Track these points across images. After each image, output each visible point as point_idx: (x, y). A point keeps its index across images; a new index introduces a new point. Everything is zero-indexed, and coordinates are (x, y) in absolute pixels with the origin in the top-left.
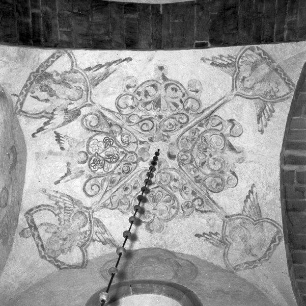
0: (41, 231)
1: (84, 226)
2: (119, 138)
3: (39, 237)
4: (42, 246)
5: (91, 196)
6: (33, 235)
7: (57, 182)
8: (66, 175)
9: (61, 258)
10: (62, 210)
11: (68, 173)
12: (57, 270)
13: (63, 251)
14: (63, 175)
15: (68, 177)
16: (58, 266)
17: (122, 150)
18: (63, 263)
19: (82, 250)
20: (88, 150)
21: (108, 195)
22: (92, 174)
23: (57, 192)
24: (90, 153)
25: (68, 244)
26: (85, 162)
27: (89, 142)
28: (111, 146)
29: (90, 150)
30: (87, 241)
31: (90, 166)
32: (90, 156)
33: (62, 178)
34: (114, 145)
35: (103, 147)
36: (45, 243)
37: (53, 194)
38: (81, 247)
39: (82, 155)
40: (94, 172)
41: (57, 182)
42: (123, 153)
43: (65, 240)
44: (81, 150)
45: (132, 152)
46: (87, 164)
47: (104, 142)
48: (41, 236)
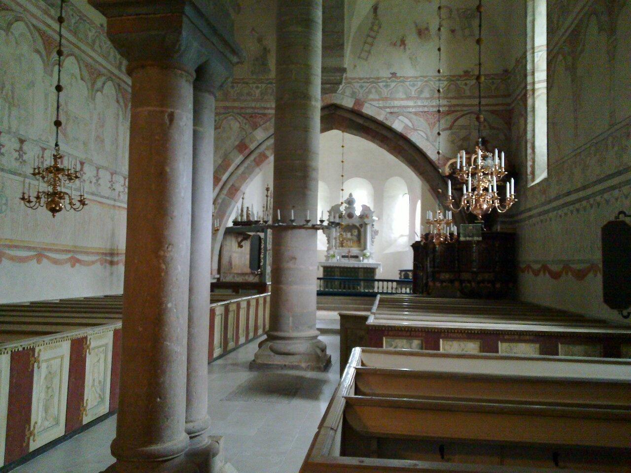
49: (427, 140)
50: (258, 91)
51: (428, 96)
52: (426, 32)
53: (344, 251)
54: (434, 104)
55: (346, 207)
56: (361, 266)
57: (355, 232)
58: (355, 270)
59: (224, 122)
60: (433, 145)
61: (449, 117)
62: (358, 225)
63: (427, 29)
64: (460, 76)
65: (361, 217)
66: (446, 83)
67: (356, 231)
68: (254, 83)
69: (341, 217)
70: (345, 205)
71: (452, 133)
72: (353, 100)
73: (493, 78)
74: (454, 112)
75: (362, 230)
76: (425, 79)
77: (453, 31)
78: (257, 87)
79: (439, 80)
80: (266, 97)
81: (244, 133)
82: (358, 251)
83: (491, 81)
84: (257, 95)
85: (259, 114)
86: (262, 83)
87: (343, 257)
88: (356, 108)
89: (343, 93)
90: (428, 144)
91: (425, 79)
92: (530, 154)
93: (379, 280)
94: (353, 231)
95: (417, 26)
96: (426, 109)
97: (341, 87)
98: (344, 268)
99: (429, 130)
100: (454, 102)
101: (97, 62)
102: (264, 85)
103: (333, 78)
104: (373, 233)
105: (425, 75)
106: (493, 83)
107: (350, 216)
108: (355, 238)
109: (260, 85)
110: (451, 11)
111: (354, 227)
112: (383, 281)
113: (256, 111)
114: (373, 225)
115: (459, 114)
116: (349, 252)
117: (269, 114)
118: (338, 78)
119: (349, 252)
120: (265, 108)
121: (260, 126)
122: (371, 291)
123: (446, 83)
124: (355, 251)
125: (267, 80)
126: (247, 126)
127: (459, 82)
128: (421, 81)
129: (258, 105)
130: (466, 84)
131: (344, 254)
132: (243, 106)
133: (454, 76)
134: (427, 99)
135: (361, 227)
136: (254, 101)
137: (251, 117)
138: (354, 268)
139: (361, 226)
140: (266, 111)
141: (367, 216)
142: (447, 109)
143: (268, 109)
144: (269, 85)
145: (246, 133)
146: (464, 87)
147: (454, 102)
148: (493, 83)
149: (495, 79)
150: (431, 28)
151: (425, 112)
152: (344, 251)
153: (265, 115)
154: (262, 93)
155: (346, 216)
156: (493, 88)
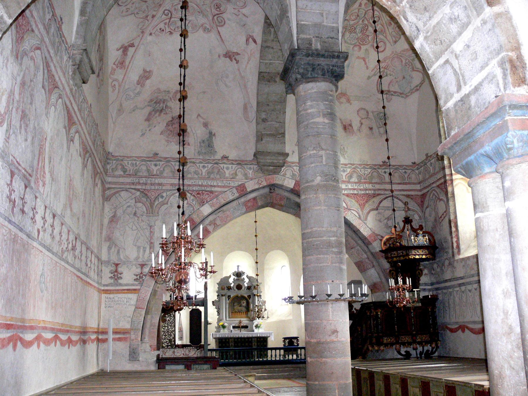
0: (392, 89)
1: (402, 61)
2: (352, 23)
3: (395, 92)
4: (401, 94)
5: (385, 49)
6: (392, 95)
7: (367, 68)
8: (364, 61)
9: (413, 85)
10: (386, 70)
11: (364, 59)
12: (418, 92)
13: (410, 82)
14: (364, 62)
15: (367, 60)
16: (417, 90)
17: (361, 21)
18: (417, 86)
19: (415, 71)
20: (353, 44)
21: (389, 37)
22: (370, 44)
23: (373, 69)
24: (355, 44)
25: (408, 77)
26: (360, 47)
27: (348, 43)
28: (355, 29)
29: (353, 43)
30: (412, 64)
31: (364, 45)
32: (358, 44)
33: (366, 64)
34: (355, 26)
35: (354, 34)
36: (399, 91)
37: (373, 73)
38: (413, 70)
39: (356, 48)
40: (369, 42)
41: (367, 68)
42: (363, 21)
43: (404, 78)
44: (351, 48)
45: (366, 13)
46: (362, 46)
47: (351, 33)
48: (394, 90)
49: (360, 218)
50: (204, 171)
51: (356, 181)
52: (350, 128)
53: (236, 321)
54: (362, 188)
55: (234, 279)
57: (244, 303)
59: (172, 197)
60: (365, 223)
61: (374, 199)
62: (246, 296)
63: (350, 125)
64: (380, 166)
65: (249, 288)
66: (369, 170)
67: (245, 301)
68: (201, 163)
69: (229, 288)
70: (233, 277)
71: (379, 213)
72: (294, 182)
73: (405, 169)
74: (378, 195)
75: (250, 301)
76: (353, 167)
77: (371, 129)
78: (204, 167)
79: (364, 168)
80: (212, 176)
81: (192, 209)
82: (248, 322)
83: (404, 171)
84: (204, 174)
85: (207, 191)
86: (208, 163)
87: (234, 327)
88: (297, 189)
89: (284, 175)
90: (361, 222)
91: (353, 167)
92: (454, 232)
93: (272, 349)
94: (242, 303)
95: (342, 123)
96: (356, 192)
97: (283, 169)
99: (360, 210)
100: (377, 187)
101: (86, 139)
102: (210, 165)
103: (276, 161)
105: (352, 163)
106: (405, 172)
107: (239, 287)
108: (244, 309)
109: (206, 165)
110: (367, 112)
111: (243, 297)
112: (276, 349)
113: (203, 188)
115: (382, 197)
116: (240, 322)
117: (216, 192)
118: (281, 161)
119: (240, 322)
120: (211, 186)
121: (207, 202)
123: (369, 170)
124: (245, 321)
125: (214, 160)
126: (194, 203)
127: (380, 170)
128: (349, 168)
129: (205, 183)
130: (385, 172)
131: (234, 325)
132: (190, 183)
133: (375, 165)
134: (356, 183)
135: (250, 298)
136: (201, 178)
137: (198, 194)
139: (249, 297)
140: (213, 189)
142: (373, 192)
143: (215, 186)
144: (216, 165)
145: (194, 209)
146: (384, 174)
147: (377, 187)
148: (405, 172)
149: (407, 169)
150: (353, 125)
151: (355, 194)
152: (236, 321)
153: (212, 192)
154: (209, 173)
155: (235, 288)
156: (406, 176)
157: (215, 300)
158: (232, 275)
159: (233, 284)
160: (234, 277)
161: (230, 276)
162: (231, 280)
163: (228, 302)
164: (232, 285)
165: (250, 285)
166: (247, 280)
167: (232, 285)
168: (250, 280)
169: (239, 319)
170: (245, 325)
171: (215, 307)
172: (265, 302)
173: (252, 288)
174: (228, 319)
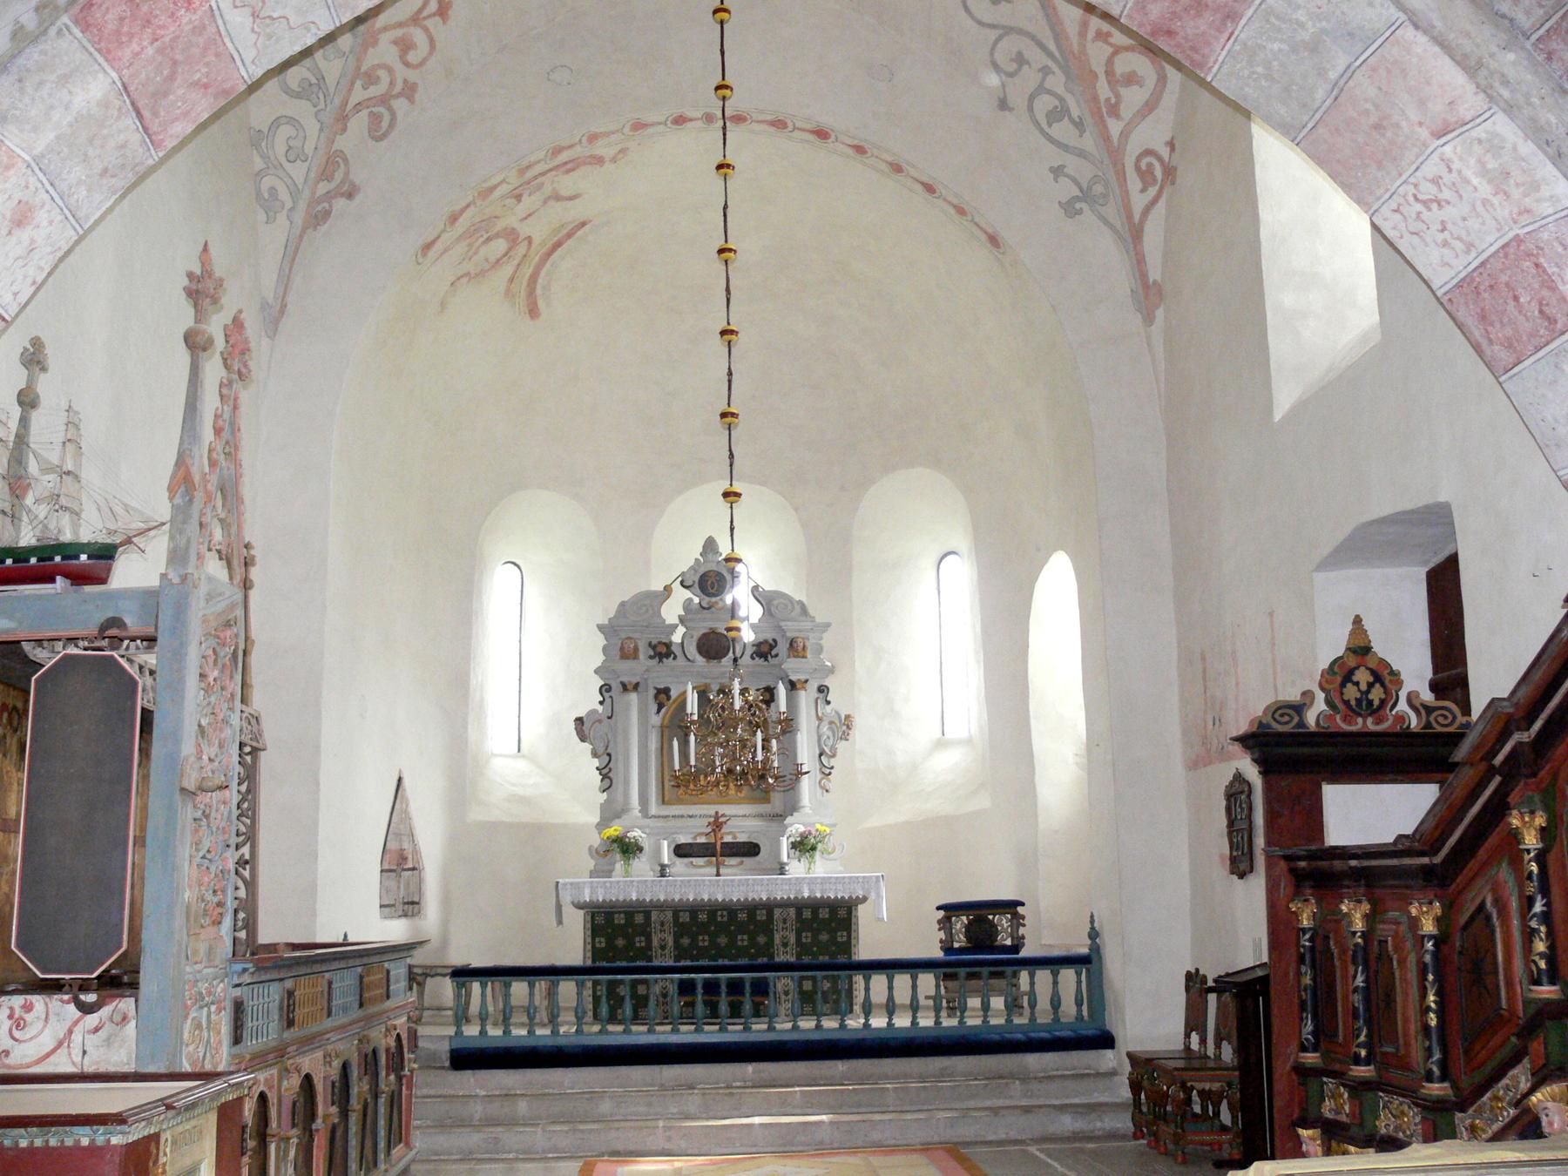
53: (693, 822)
55: (687, 605)
56: (780, 894)
58: (751, 920)
65: (764, 650)
69: (663, 651)
70: (681, 595)
87: (681, 851)
98: (694, 909)
104: (825, 729)
107: (714, 646)
114: (822, 689)
116: (717, 824)
119: (717, 824)
122: (830, 1023)
124: (742, 821)
131: (683, 839)
138: (752, 908)
141: (795, 649)
155: (692, 650)
157: (594, 712)
158: (677, 586)
159: (681, 630)
160: (687, 594)
161: (668, 589)
162: (671, 612)
163: (656, 720)
164: (677, 638)
165: (769, 636)
166: (751, 611)
167: (677, 638)
168: (768, 612)
169: (710, 810)
170: (742, 838)
171: (587, 747)
172: (848, 722)
173: (782, 648)
174: (654, 809)
